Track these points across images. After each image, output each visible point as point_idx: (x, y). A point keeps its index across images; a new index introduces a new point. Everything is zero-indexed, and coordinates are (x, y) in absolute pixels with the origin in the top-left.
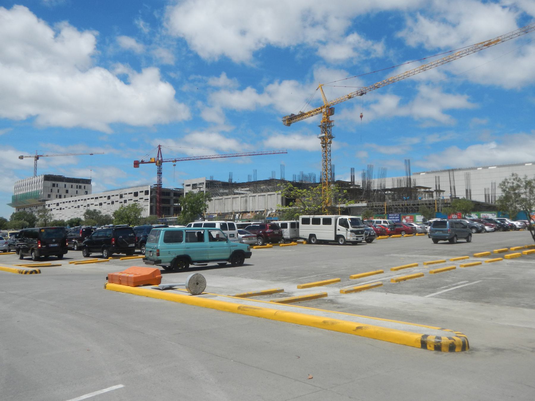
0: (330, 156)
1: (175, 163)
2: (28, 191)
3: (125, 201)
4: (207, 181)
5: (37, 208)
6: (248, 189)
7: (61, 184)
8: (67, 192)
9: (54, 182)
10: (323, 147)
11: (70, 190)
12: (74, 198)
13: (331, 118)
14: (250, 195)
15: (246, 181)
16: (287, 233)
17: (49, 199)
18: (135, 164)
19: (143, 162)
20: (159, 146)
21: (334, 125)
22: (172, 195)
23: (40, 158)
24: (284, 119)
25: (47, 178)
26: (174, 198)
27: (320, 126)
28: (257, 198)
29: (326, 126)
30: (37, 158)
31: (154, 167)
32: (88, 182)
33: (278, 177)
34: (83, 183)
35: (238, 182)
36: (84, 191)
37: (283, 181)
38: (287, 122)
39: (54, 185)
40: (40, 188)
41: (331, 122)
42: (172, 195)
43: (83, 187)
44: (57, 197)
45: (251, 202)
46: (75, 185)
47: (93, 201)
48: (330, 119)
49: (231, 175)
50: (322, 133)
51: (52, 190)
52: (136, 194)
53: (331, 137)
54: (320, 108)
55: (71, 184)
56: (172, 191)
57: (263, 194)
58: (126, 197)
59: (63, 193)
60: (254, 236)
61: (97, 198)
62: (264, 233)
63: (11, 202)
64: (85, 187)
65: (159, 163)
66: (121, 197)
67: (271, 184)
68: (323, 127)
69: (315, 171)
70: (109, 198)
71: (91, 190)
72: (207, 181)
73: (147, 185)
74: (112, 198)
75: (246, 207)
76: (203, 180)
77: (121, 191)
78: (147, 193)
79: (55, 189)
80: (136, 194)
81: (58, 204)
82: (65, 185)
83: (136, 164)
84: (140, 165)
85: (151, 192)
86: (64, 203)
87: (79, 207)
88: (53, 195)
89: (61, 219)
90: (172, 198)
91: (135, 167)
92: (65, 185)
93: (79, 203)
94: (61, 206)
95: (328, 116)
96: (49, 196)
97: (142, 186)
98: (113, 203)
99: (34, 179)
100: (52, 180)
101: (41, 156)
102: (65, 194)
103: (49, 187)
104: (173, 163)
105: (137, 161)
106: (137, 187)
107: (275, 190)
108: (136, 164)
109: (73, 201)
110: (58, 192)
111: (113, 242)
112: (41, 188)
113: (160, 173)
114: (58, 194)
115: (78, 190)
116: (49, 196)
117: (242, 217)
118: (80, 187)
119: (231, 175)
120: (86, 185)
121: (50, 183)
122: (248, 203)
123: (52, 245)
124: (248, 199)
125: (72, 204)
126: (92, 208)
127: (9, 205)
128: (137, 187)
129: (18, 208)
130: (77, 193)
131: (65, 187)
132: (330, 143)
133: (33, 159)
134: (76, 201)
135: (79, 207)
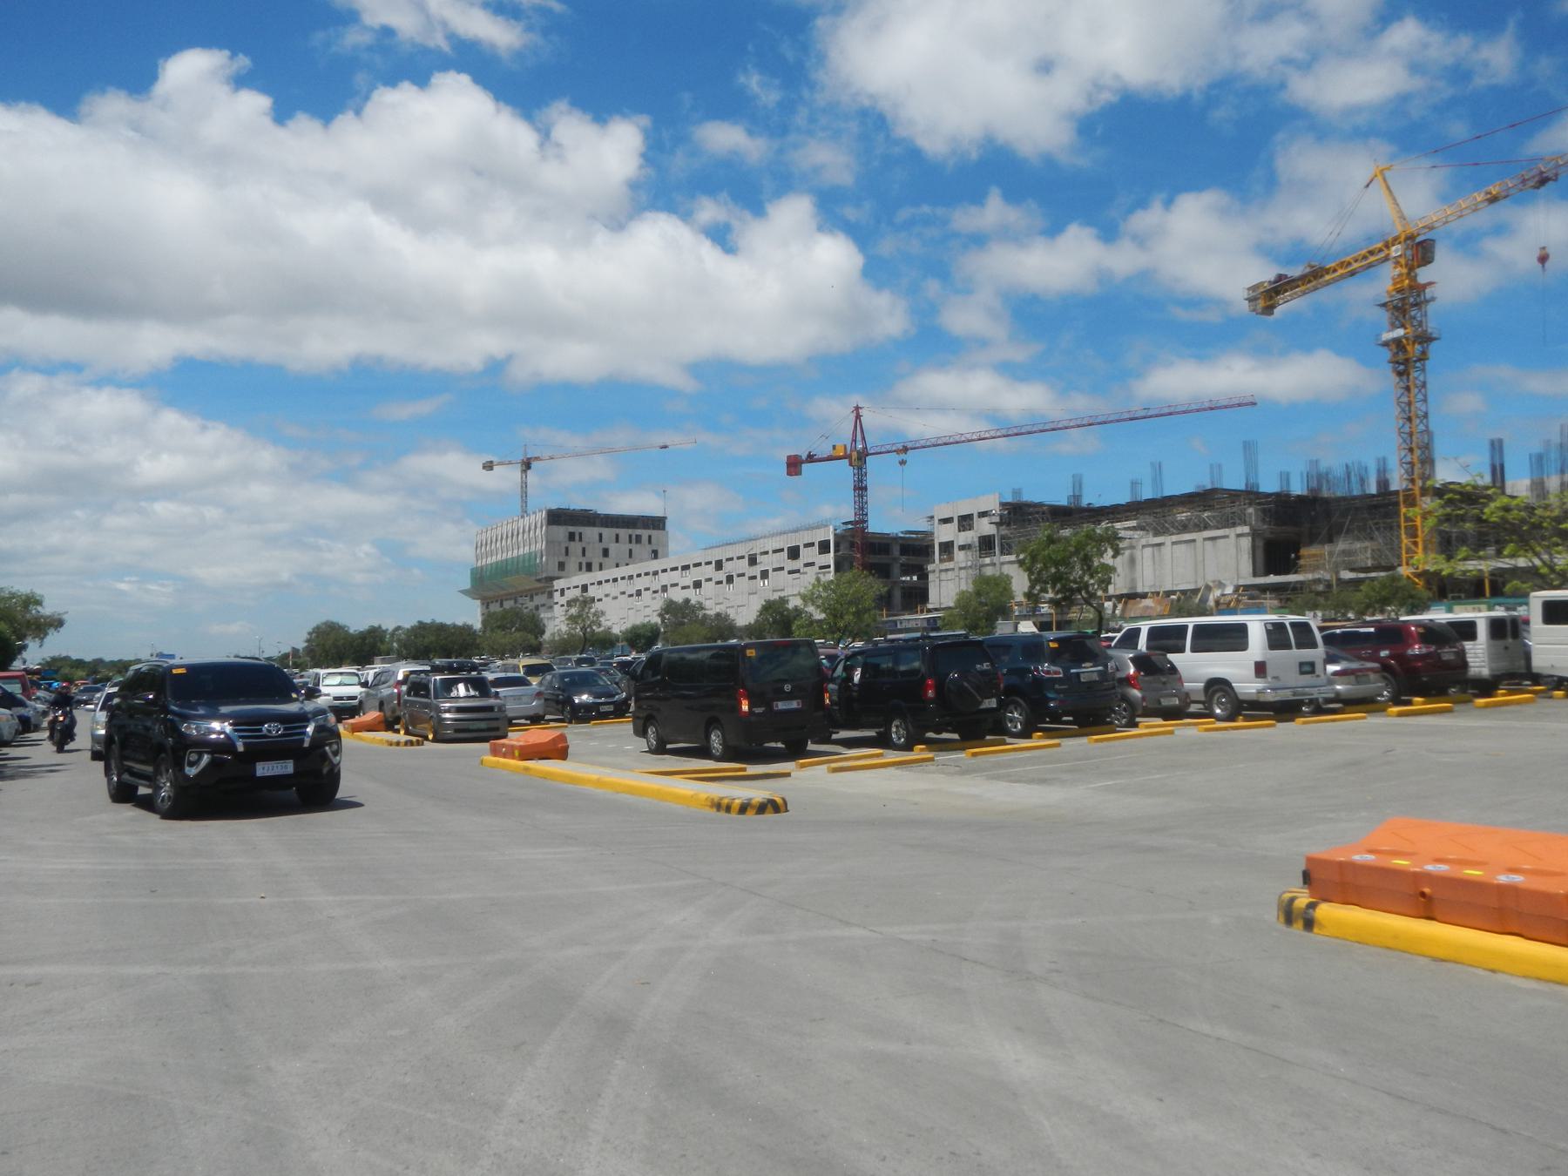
0: (1425, 400)
1: (903, 456)
4: (1003, 505)
5: (532, 599)
6: (1133, 523)
7: (590, 533)
8: (606, 553)
9: (571, 529)
10: (1400, 374)
11: (613, 547)
13: (1424, 275)
14: (1143, 542)
15: (1123, 498)
16: (1479, 656)
19: (811, 458)
20: (857, 408)
21: (1433, 299)
22: (896, 551)
23: (534, 464)
24: (1252, 294)
25: (556, 517)
26: (903, 559)
27: (1384, 305)
28: (1167, 550)
29: (1408, 302)
30: (527, 465)
31: (844, 470)
32: (657, 523)
33: (1234, 480)
34: (644, 530)
35: (1098, 502)
36: (649, 548)
37: (1251, 495)
38: (1261, 304)
39: (572, 537)
41: (1424, 286)
42: (896, 551)
43: (645, 539)
45: (1148, 563)
46: (624, 533)
47: (675, 577)
48: (1422, 280)
49: (1078, 483)
50: (1393, 327)
52: (794, 553)
53: (1425, 339)
54: (1379, 245)
56: (896, 539)
57: (1187, 537)
58: (766, 562)
59: (595, 556)
60: (1372, 670)
61: (686, 568)
62: (1401, 658)
63: (467, 585)
65: (859, 458)
66: (753, 561)
67: (1208, 506)
68: (1396, 308)
69: (1364, 453)
70: (719, 565)
71: (666, 545)
72: (1003, 505)
73: (822, 525)
74: (728, 566)
75: (1133, 581)
76: (992, 503)
77: (751, 544)
78: (824, 547)
79: (576, 547)
80: (794, 553)
83: (794, 465)
84: (805, 467)
85: (837, 545)
86: (600, 583)
87: (639, 593)
88: (572, 564)
89: (628, 625)
90: (895, 559)
91: (789, 474)
93: (640, 584)
95: (1411, 269)
96: (562, 566)
98: (730, 579)
100: (565, 523)
101: (537, 459)
102: (601, 559)
104: (895, 458)
106: (796, 531)
107: (1229, 522)
108: (794, 465)
111: (930, 693)
112: (541, 546)
113: (860, 489)
115: (633, 546)
116: (562, 566)
117: (1123, 611)
118: (639, 539)
119: (1078, 483)
120: (654, 533)
121: (561, 532)
122: (1139, 567)
123: (781, 705)
124: (1138, 553)
125: (622, 585)
126: (678, 596)
127: (464, 592)
128: (796, 531)
129: (486, 602)
132: (1423, 357)
134: (631, 577)
135: (639, 593)
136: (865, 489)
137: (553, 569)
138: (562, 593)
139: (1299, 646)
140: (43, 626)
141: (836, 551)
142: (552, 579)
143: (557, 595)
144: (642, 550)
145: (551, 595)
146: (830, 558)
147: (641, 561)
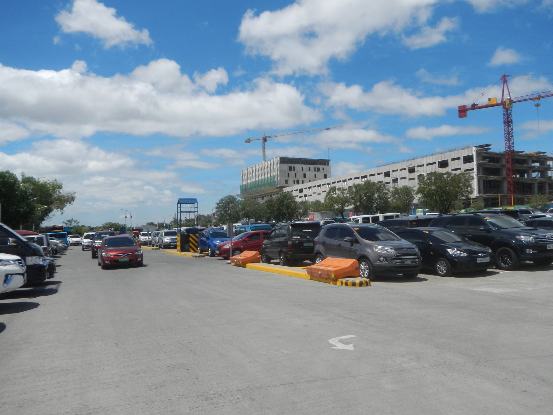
1: (537, 102)
2: (260, 178)
3: (395, 181)
5: (263, 199)
7: (298, 167)
8: (305, 176)
9: (290, 165)
11: (308, 173)
12: (311, 184)
17: (287, 185)
18: (460, 111)
19: (474, 107)
23: (268, 140)
25: (283, 160)
30: (265, 140)
32: (325, 162)
34: (320, 164)
39: (290, 169)
40: (276, 173)
43: (321, 169)
46: (312, 167)
51: (288, 174)
55: (308, 166)
59: (300, 177)
64: (323, 169)
71: (330, 172)
74: (393, 175)
77: (410, 162)
78: (468, 159)
79: (292, 173)
81: (301, 191)
82: (302, 168)
88: (291, 181)
92: (302, 168)
94: (305, 192)
96: (286, 182)
97: (455, 150)
99: (266, 164)
102: (303, 179)
103: (285, 171)
105: (465, 106)
109: (314, 187)
112: (277, 173)
114: (296, 179)
115: (316, 173)
116: (286, 182)
120: (325, 167)
121: (286, 166)
131: (303, 170)
133: (262, 141)
136: (511, 122)
137: (283, 183)
140: (64, 202)
141: (477, 161)
142: (282, 188)
144: (320, 174)
146: (474, 165)
147: (320, 179)
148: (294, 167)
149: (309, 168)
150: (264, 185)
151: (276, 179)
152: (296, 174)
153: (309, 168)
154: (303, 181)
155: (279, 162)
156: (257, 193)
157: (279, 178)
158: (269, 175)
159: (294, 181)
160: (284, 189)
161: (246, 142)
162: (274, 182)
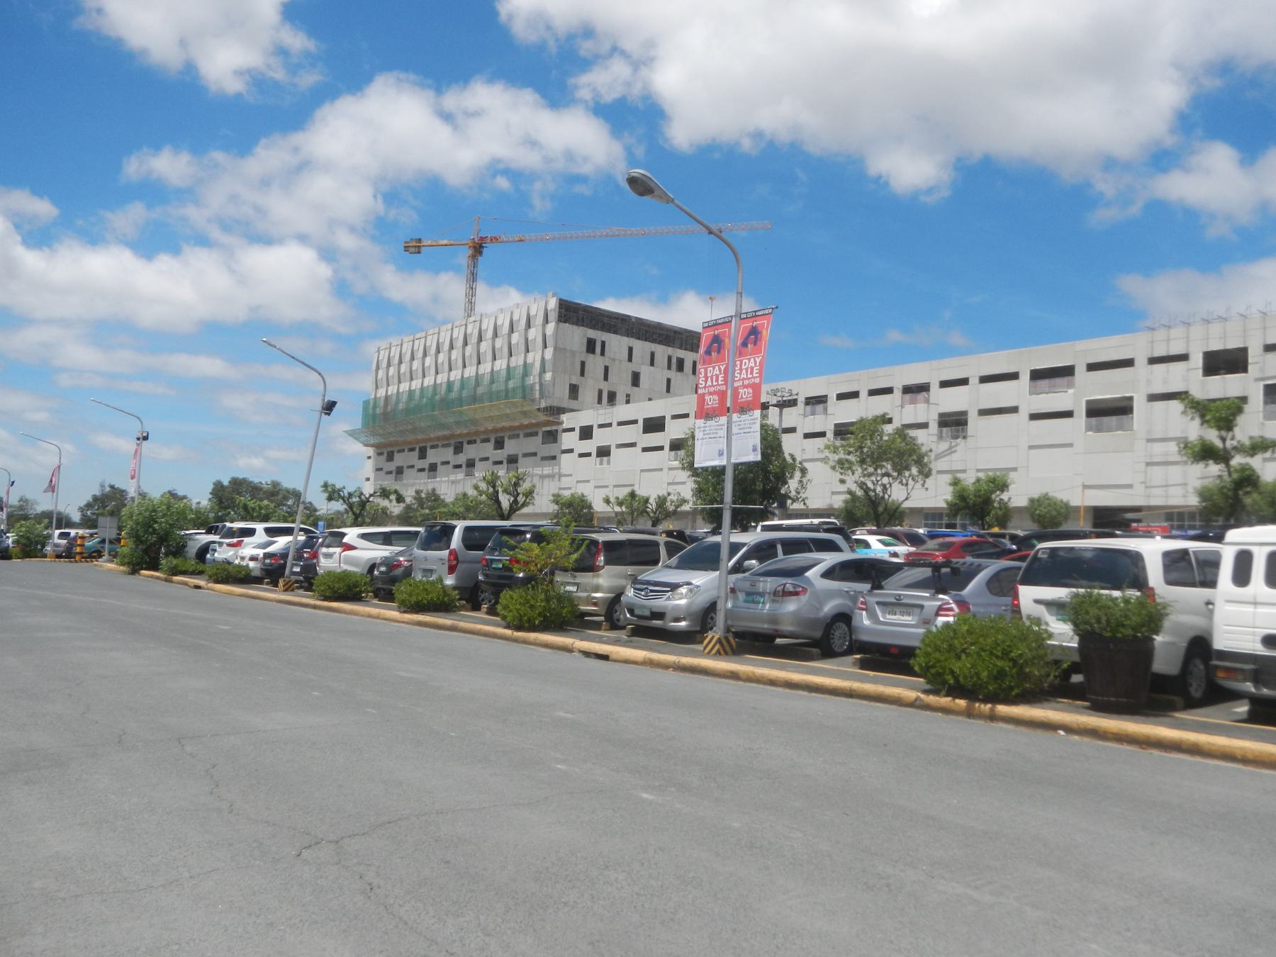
2: (456, 375)
7: (617, 344)
9: (592, 333)
11: (646, 372)
17: (573, 404)
25: (570, 313)
39: (591, 346)
40: (534, 357)
43: (688, 366)
44: (600, 401)
46: (662, 351)
51: (583, 364)
79: (595, 364)
81: (654, 425)
82: (631, 350)
88: (588, 394)
92: (631, 350)
96: (574, 390)
100: (580, 322)
101: (495, 239)
103: (573, 353)
110: (606, 378)
114: (606, 388)
115: (673, 374)
116: (574, 390)
121: (577, 335)
130: (668, 390)
131: (630, 359)
137: (561, 396)
138: (586, 433)
139: (1211, 583)
142: (561, 410)
143: (569, 440)
145: (552, 437)
148: (603, 344)
149: (653, 355)
150: (474, 399)
151: (533, 379)
152: (606, 369)
153: (653, 355)
154: (628, 396)
155: (553, 316)
156: (443, 426)
157: (548, 376)
158: (501, 364)
159: (600, 392)
160: (564, 417)
161: (406, 248)
162: (525, 391)
